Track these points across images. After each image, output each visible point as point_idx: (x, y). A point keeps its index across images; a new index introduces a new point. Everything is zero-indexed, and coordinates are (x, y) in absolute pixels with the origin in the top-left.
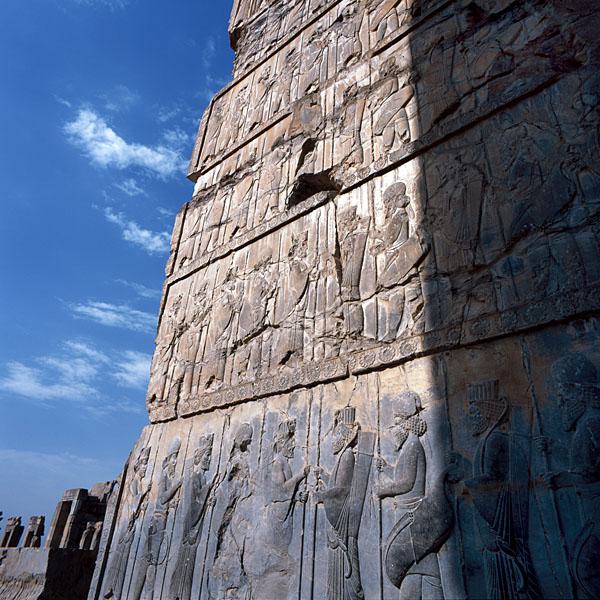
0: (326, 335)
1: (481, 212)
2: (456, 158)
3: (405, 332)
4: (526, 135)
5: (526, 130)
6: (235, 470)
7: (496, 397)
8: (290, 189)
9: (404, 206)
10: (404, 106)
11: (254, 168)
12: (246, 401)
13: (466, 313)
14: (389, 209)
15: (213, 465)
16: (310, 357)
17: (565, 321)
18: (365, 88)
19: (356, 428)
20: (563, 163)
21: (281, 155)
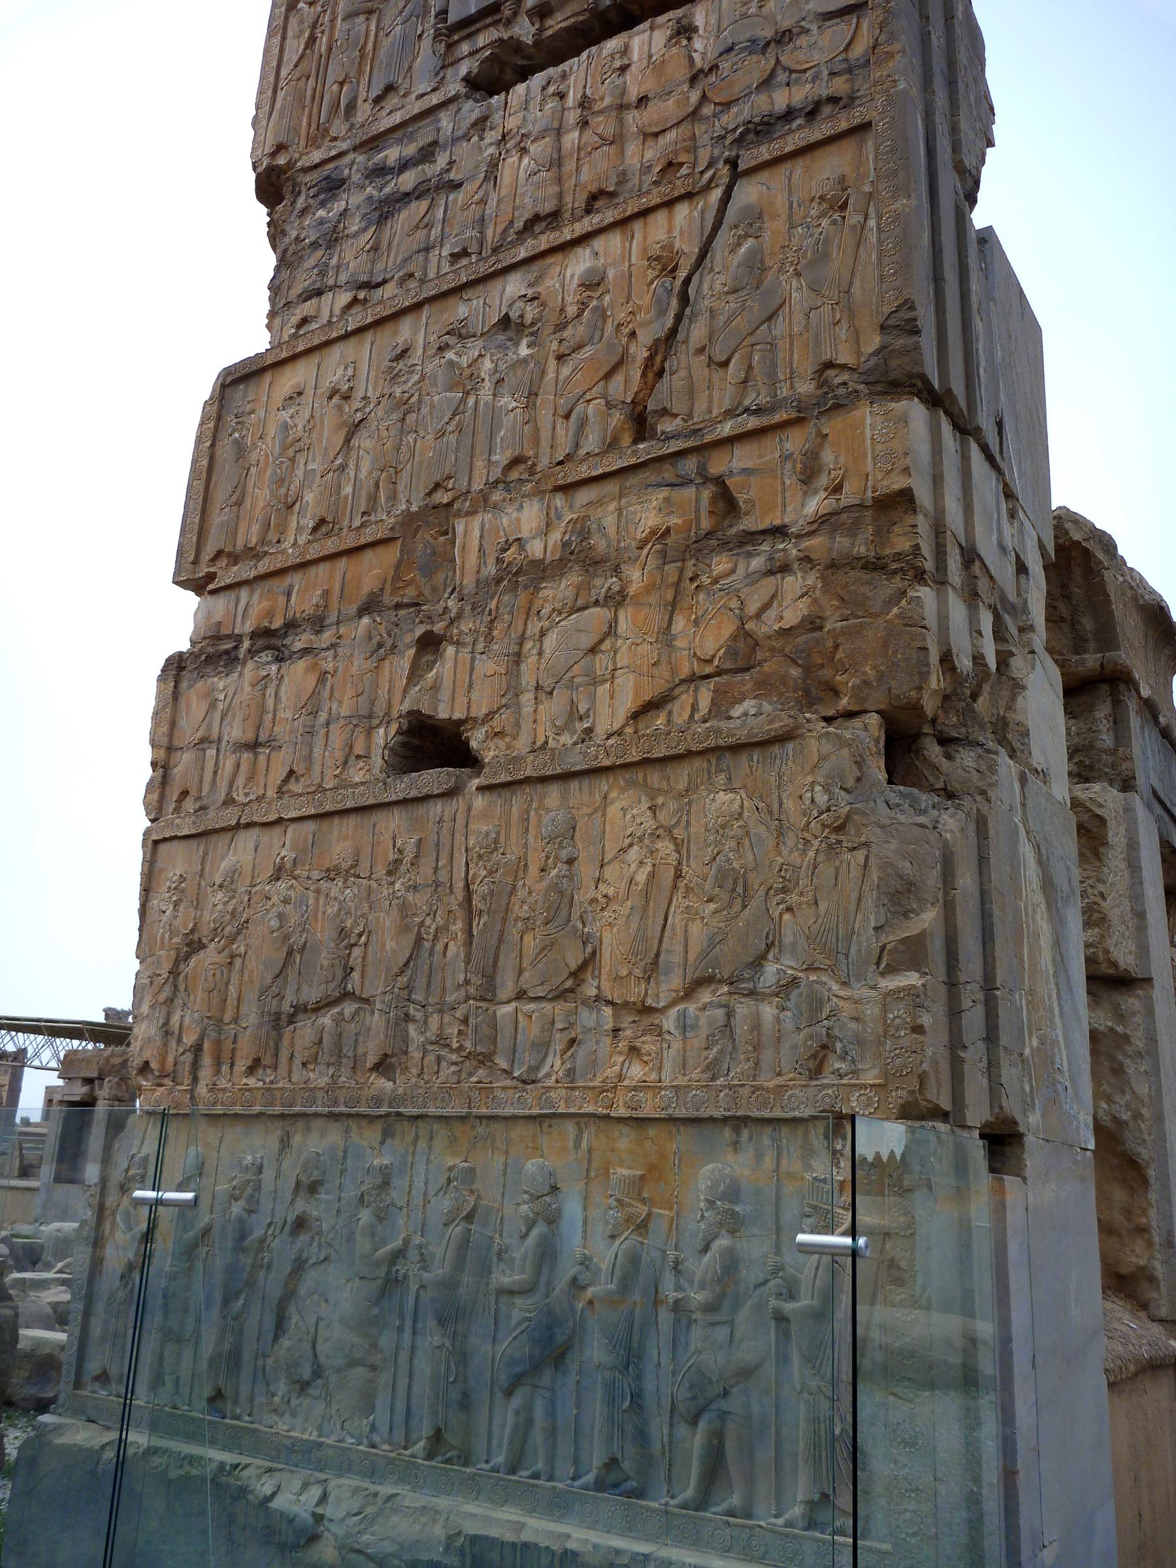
0: (441, 1041)
1: (666, 920)
2: (650, 808)
3: (548, 1075)
4: (740, 814)
5: (742, 807)
7: (639, 1195)
8: (394, 727)
9: (570, 861)
10: (593, 650)
13: (624, 1071)
14: (548, 858)
15: (266, 1206)
16: (415, 1071)
17: (725, 1120)
19: (472, 1199)
20: (770, 889)
21: (376, 639)
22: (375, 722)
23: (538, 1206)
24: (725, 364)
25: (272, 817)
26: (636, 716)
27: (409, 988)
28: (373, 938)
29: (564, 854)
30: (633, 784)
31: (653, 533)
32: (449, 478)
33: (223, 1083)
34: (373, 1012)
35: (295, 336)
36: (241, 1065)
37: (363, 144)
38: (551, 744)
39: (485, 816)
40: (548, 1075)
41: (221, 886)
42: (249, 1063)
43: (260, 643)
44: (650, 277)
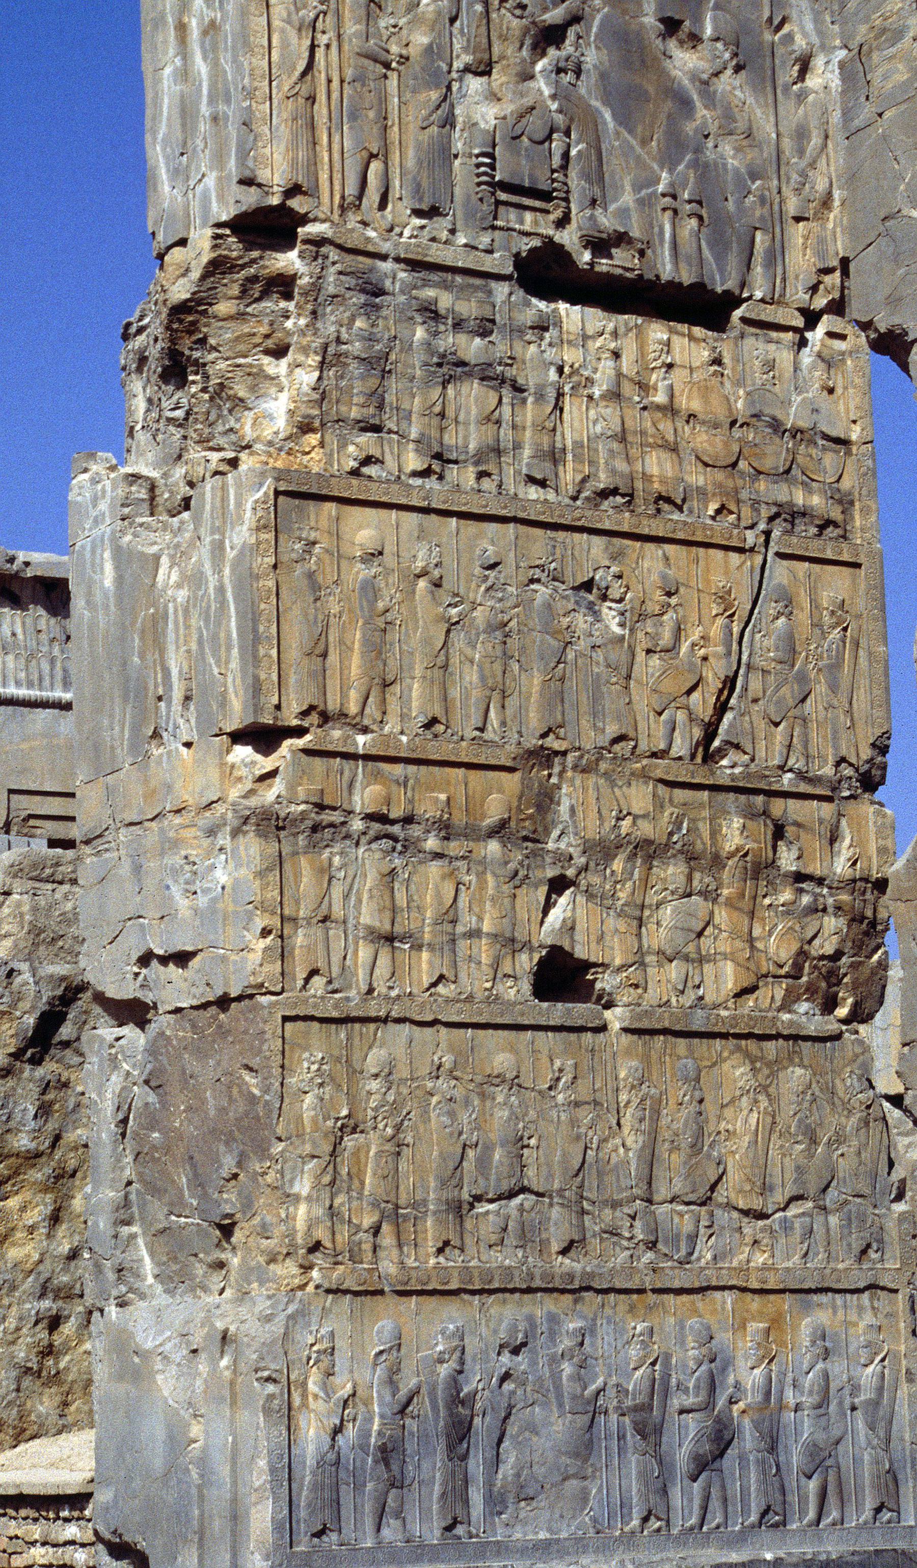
6: (506, 1377)
9: (701, 1101)
11: (455, 847)
12: (513, 1291)
18: (649, 842)
22: (518, 946)
23: (704, 1350)
24: (777, 725)
25: (429, 1018)
26: (737, 995)
27: (581, 1187)
28: (543, 1144)
29: (697, 1095)
30: (738, 1048)
31: (737, 850)
32: (560, 727)
33: (411, 1262)
34: (551, 1205)
35: (355, 473)
36: (431, 1246)
37: (407, 261)
38: (674, 1000)
39: (628, 1052)
40: (699, 1259)
41: (376, 1076)
42: (440, 1245)
43: (376, 826)
44: (714, 612)
